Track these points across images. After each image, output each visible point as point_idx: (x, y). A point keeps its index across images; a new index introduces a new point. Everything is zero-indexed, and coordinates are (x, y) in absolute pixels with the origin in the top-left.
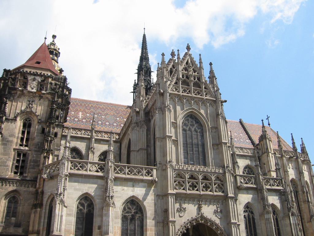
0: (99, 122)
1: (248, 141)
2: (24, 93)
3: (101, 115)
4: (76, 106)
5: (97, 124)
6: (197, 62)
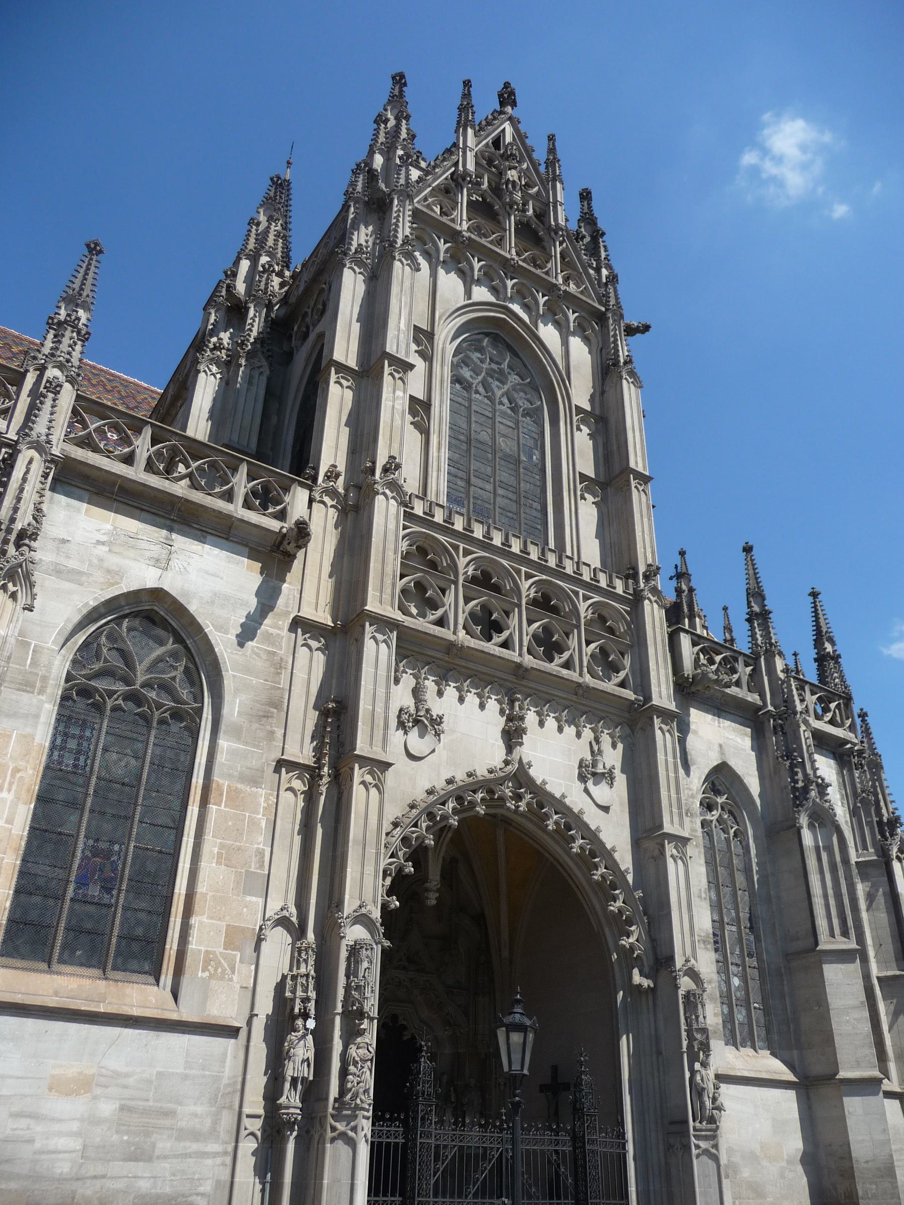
6: (540, 155)
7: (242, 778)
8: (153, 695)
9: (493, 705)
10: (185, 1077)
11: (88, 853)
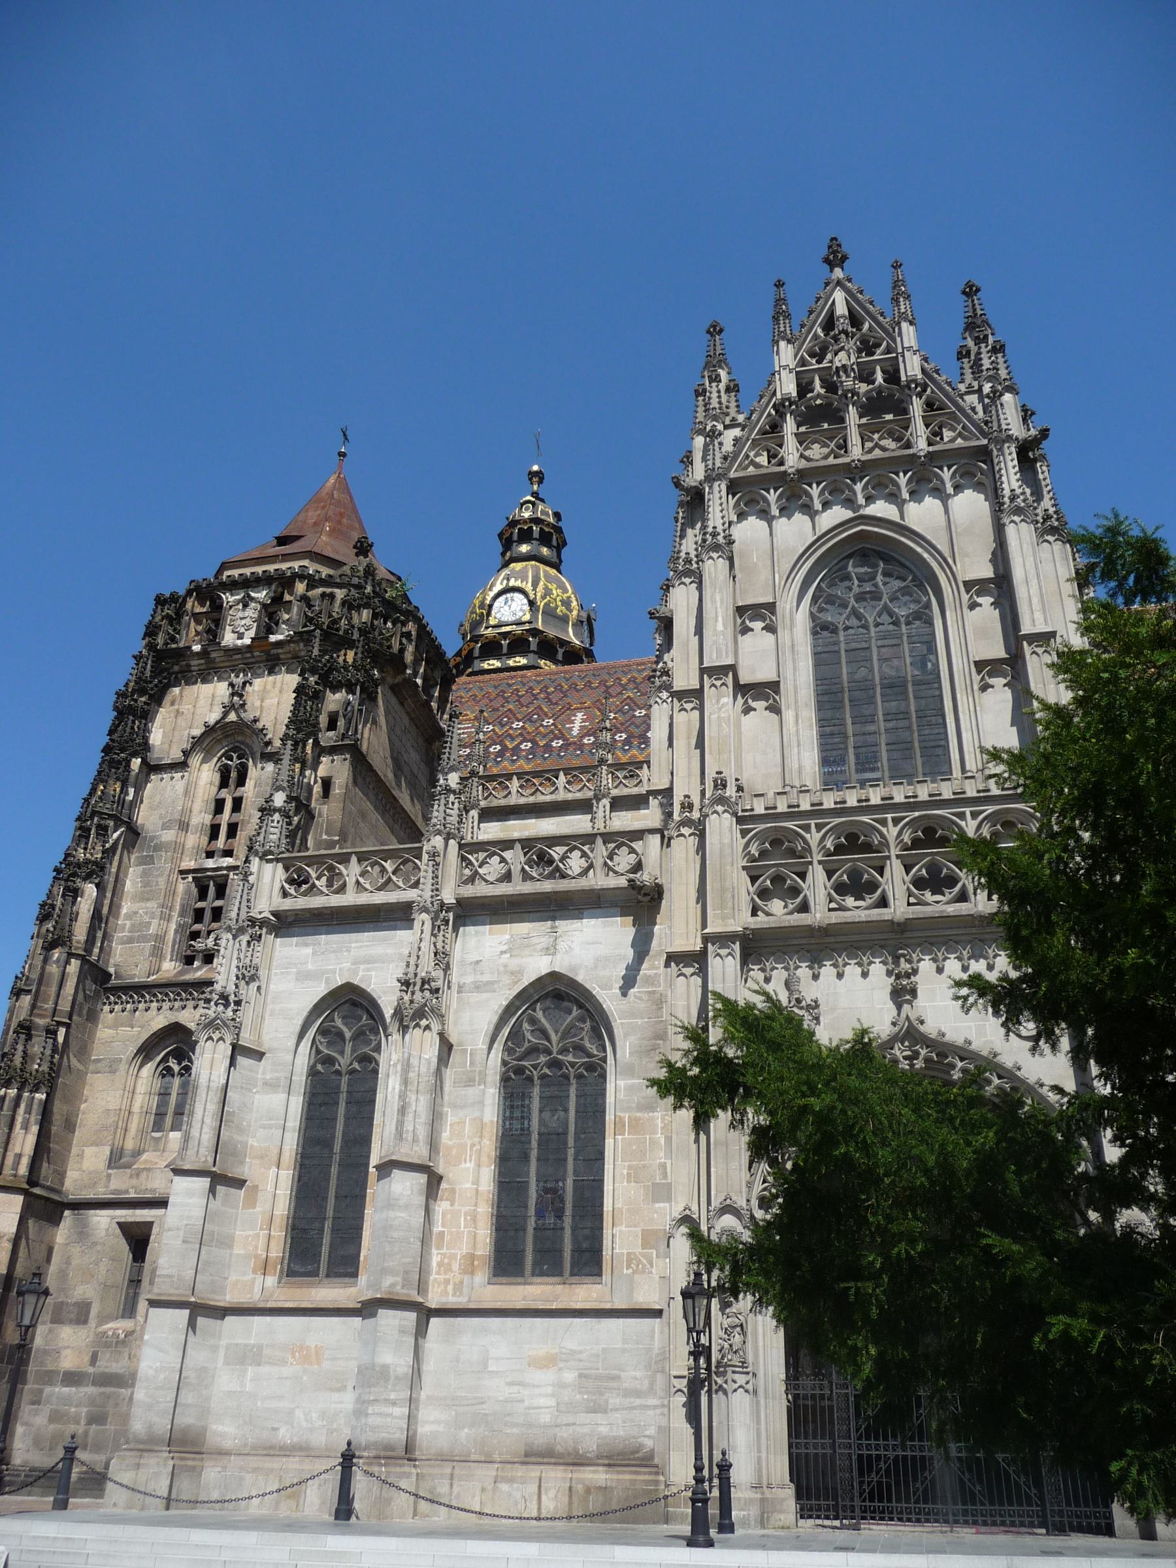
2: (213, 661)
4: (566, 696)
5: (641, 743)
9: (878, 969)
10: (624, 1351)
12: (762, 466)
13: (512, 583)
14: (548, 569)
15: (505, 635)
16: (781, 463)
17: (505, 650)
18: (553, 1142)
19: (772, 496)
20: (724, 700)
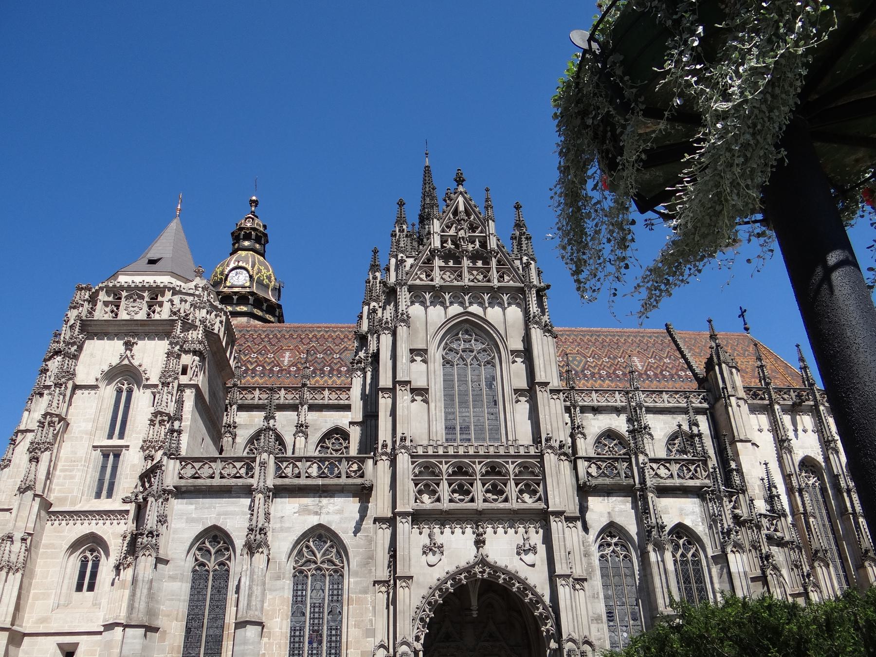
0: (325, 369)
1: (684, 374)
3: (331, 353)
4: (279, 341)
5: (321, 374)
7: (360, 592)
8: (325, 566)
9: (469, 531)
11: (311, 632)
12: (423, 280)
13: (241, 264)
14: (259, 256)
15: (236, 293)
16: (432, 280)
17: (235, 301)
18: (317, 608)
19: (427, 296)
20: (406, 397)
